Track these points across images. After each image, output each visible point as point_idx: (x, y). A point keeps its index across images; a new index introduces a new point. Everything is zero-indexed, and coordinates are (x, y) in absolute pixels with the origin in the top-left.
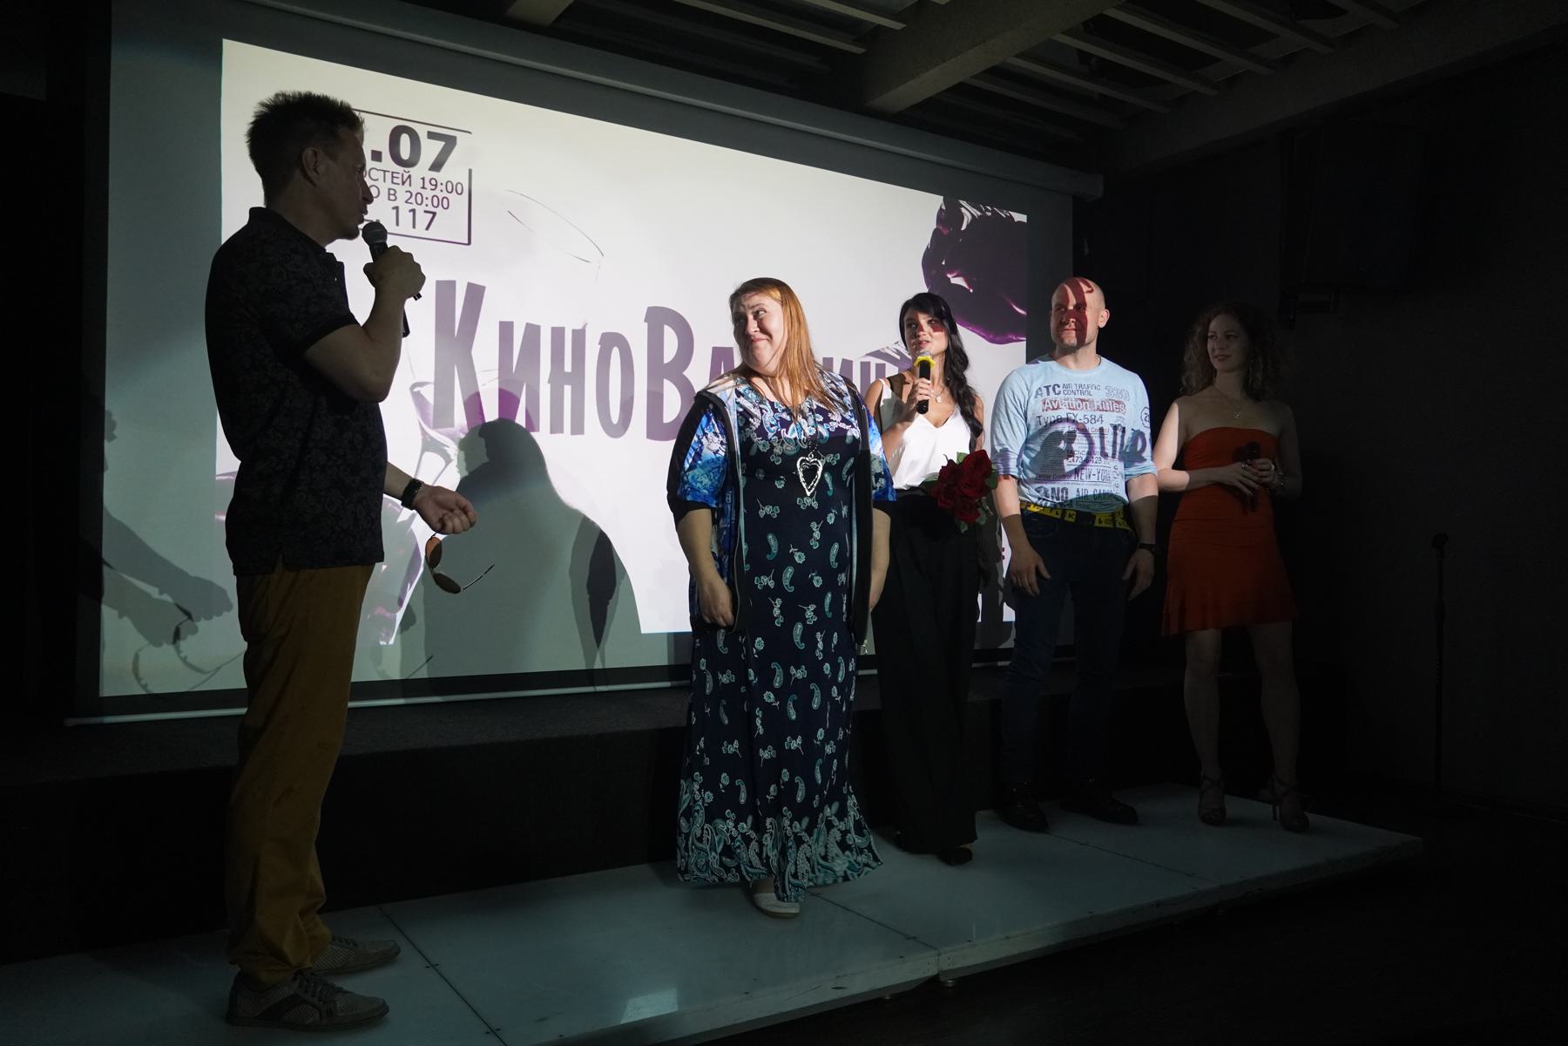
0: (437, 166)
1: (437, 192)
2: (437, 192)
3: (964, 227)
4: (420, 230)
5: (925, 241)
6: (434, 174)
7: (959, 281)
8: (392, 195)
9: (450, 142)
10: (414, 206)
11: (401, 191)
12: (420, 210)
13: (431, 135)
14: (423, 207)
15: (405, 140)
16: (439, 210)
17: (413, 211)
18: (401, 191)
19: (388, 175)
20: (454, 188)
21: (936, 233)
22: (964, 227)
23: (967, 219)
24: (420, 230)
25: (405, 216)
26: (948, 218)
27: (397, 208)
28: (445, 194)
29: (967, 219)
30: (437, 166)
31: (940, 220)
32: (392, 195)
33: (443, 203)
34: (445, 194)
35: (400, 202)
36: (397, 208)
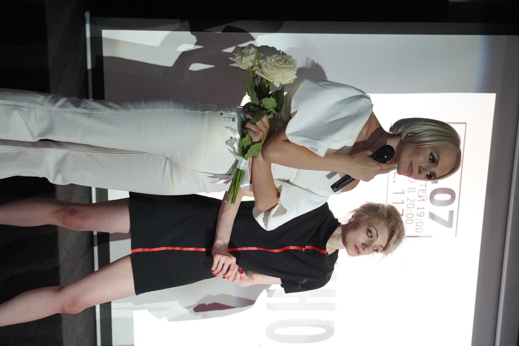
0: (432, 216)
1: (416, 217)
2: (416, 217)
6: (427, 215)
9: (449, 224)
13: (451, 213)
15: (448, 197)
17: (403, 203)
18: (415, 195)
19: (424, 188)
27: (404, 193)
30: (432, 216)
36: (404, 193)
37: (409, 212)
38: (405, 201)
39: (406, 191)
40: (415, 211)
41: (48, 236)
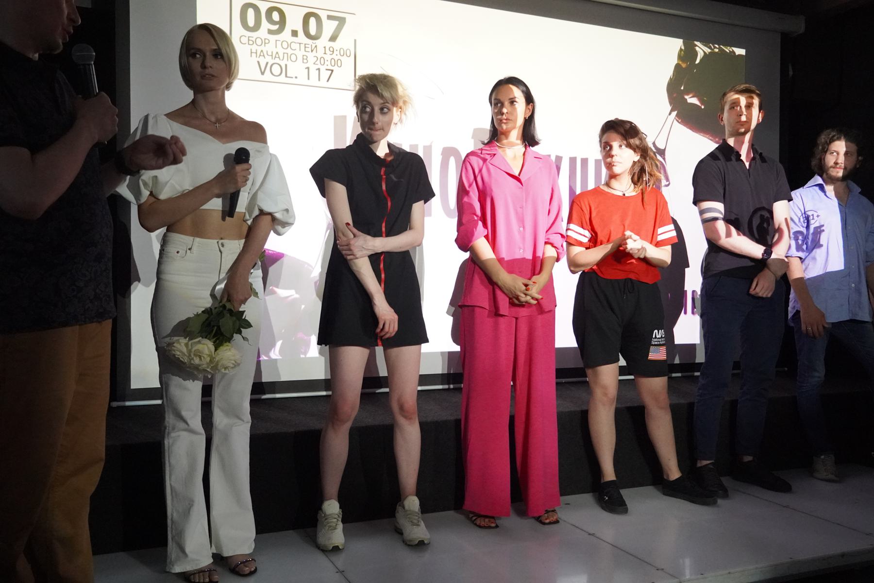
1: (334, 56)
2: (334, 56)
3: (698, 61)
4: (323, 82)
5: (669, 72)
7: (693, 100)
8: (305, 59)
10: (319, 66)
11: (311, 57)
12: (323, 69)
14: (325, 67)
16: (335, 68)
17: (319, 69)
18: (311, 57)
20: (345, 54)
21: (677, 67)
22: (698, 61)
23: (700, 55)
24: (323, 82)
25: (314, 73)
26: (687, 54)
27: (308, 68)
28: (339, 57)
29: (700, 55)
31: (680, 57)
32: (305, 59)
33: (337, 63)
34: (339, 57)
35: (310, 64)
36: (308, 68)
37: (329, 63)
38: (317, 67)
39: (307, 65)
40: (328, 57)
41: (358, 435)
